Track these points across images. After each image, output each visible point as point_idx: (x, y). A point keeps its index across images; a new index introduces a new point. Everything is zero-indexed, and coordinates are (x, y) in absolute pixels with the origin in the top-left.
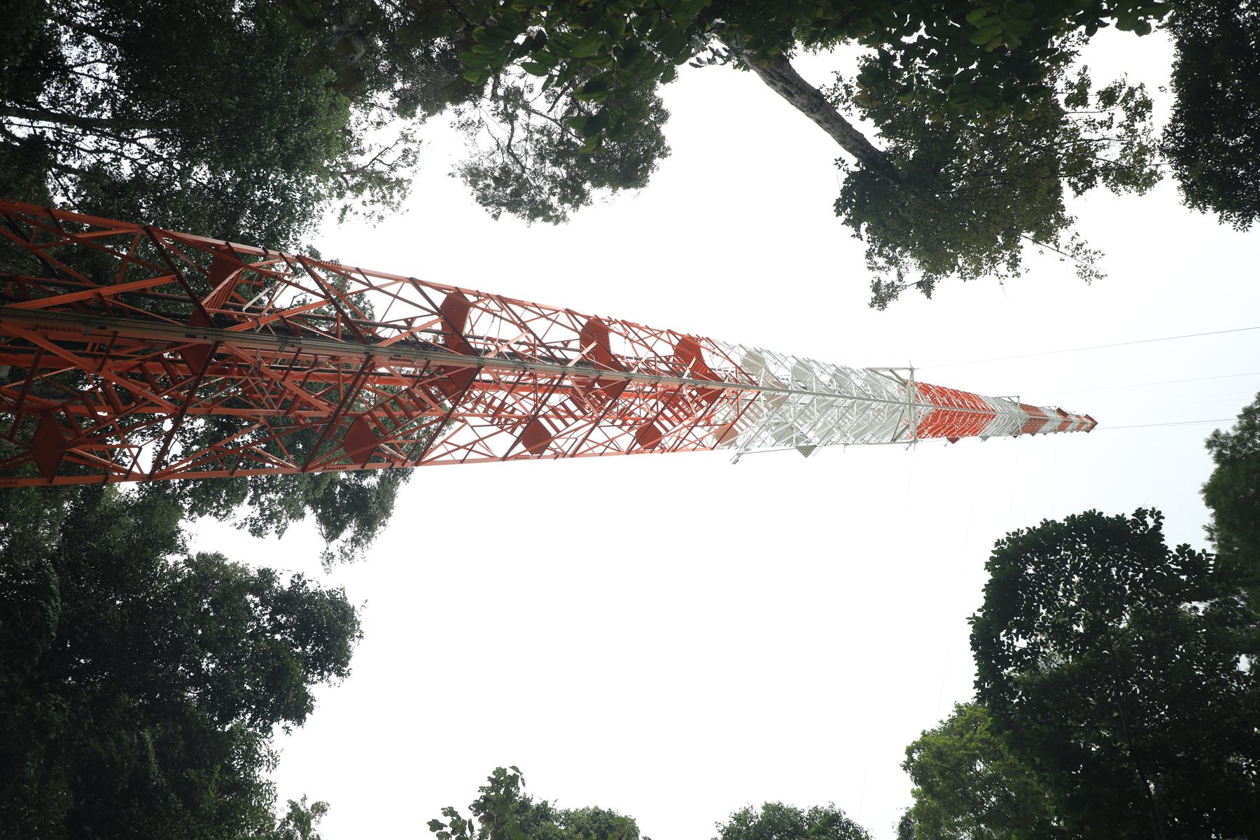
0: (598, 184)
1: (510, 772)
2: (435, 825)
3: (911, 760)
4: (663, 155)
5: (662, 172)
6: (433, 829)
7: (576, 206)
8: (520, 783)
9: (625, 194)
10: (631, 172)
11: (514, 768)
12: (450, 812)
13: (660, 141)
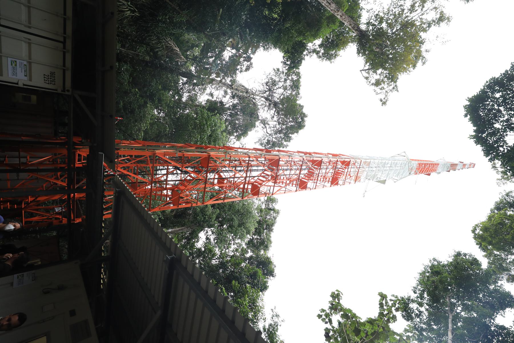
0: (293, 133)
1: (336, 293)
2: (320, 316)
3: (475, 234)
4: (306, 117)
5: (308, 121)
6: (319, 318)
7: (289, 141)
8: (341, 295)
9: (301, 132)
10: (299, 126)
11: (337, 291)
12: (323, 310)
13: (304, 114)
